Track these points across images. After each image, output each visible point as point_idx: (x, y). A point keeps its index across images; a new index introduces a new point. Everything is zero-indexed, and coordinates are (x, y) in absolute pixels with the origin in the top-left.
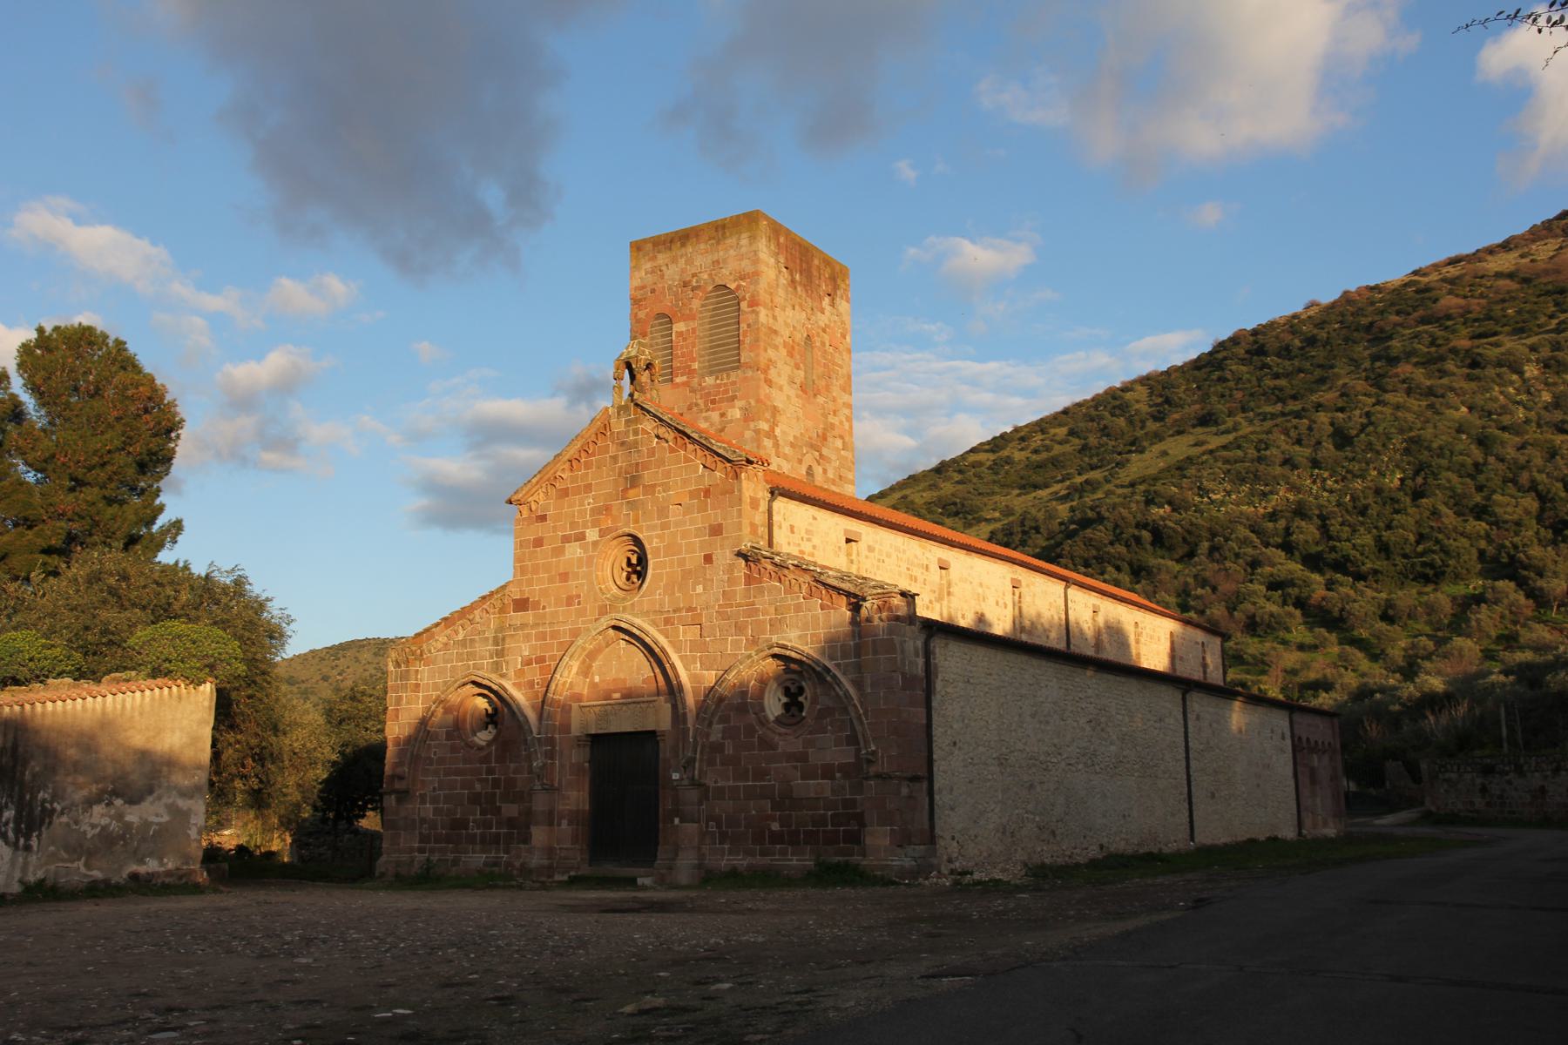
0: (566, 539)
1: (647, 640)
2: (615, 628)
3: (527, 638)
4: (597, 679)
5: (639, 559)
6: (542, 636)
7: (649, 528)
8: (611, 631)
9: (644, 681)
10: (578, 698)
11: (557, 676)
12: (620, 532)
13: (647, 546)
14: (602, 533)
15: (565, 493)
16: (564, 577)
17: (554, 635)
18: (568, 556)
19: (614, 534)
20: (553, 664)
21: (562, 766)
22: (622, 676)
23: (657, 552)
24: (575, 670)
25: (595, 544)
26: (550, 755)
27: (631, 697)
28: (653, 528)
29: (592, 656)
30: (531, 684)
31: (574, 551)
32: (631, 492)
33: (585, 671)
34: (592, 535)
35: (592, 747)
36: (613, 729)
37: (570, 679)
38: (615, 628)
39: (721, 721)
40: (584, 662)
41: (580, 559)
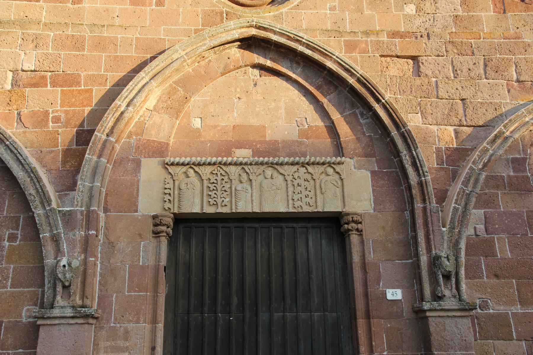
1: (329, 64)
2: (248, 43)
3: (37, 42)
4: (197, 123)
6: (78, 44)
8: (235, 53)
9: (303, 133)
10: (159, 150)
11: (121, 103)
17: (100, 44)
20: (98, 92)
21: (110, 272)
22: (253, 121)
24: (151, 103)
26: (87, 246)
27: (271, 157)
29: (189, 85)
30: (41, 119)
33: (174, 105)
35: (172, 242)
36: (245, 206)
37: (145, 111)
38: (248, 43)
39: (485, 202)
40: (171, 93)
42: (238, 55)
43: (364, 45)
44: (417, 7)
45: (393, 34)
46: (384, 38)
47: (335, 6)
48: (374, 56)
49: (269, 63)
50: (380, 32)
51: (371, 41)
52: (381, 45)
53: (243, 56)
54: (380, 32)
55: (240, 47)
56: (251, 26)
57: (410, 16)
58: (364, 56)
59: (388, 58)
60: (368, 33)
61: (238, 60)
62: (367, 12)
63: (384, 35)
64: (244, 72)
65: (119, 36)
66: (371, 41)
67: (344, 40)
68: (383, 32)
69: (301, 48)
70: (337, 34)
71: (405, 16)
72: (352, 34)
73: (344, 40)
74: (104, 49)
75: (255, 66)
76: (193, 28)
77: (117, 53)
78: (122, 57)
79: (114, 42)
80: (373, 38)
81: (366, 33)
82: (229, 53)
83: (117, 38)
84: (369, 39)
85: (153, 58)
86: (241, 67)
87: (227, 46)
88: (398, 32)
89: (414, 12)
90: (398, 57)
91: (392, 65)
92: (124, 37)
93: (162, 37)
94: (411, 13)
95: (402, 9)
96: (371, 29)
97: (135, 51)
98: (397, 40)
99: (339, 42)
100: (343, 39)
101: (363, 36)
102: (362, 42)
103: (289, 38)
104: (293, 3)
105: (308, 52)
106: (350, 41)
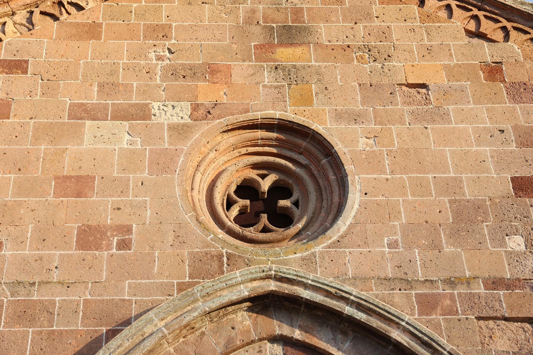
0: (82, 112)
1: (396, 335)
2: (263, 304)
5: (280, 190)
7: (339, 116)
8: (244, 320)
12: (258, 115)
13: (339, 147)
14: (202, 113)
15: (92, 31)
16: (77, 185)
18: (87, 143)
19: (241, 118)
23: (372, 162)
25: (179, 131)
28: (356, 118)
31: (106, 142)
32: (285, 54)
34: (170, 113)
38: (263, 304)
41: (131, 160)
42: (248, 322)
43: (448, 302)
44: (526, 241)
45: (494, 283)
46: (480, 289)
47: (396, 241)
48: (467, 319)
49: (298, 334)
50: (472, 281)
51: (459, 294)
52: (476, 301)
53: (255, 324)
54: (472, 281)
55: (250, 309)
56: (268, 277)
57: (518, 254)
58: (450, 320)
59: (491, 323)
60: (453, 282)
61: (249, 331)
62: (448, 249)
63: (479, 284)
64: (257, 349)
65: (57, 299)
66: (459, 294)
67: (416, 294)
68: (477, 280)
69: (348, 310)
70: (404, 285)
71: (509, 254)
72: (428, 284)
73: (416, 294)
74: (32, 321)
75: (274, 339)
76: (175, 282)
77: (52, 326)
78: (61, 333)
79: (47, 309)
80: (462, 290)
81: (451, 282)
82: (233, 319)
83: (53, 303)
84: (456, 292)
85: (112, 333)
86: (253, 342)
87: (230, 309)
88: (502, 279)
89: (523, 247)
90: (506, 319)
91: (498, 333)
92: (64, 300)
93: (127, 298)
94: (518, 249)
95: (503, 244)
96: (457, 275)
97: (82, 322)
98: (501, 293)
99: (408, 296)
100: (413, 292)
101: (446, 287)
102: (445, 296)
103: (328, 294)
104: (330, 238)
105: (361, 316)
106: (426, 295)
